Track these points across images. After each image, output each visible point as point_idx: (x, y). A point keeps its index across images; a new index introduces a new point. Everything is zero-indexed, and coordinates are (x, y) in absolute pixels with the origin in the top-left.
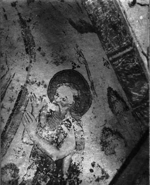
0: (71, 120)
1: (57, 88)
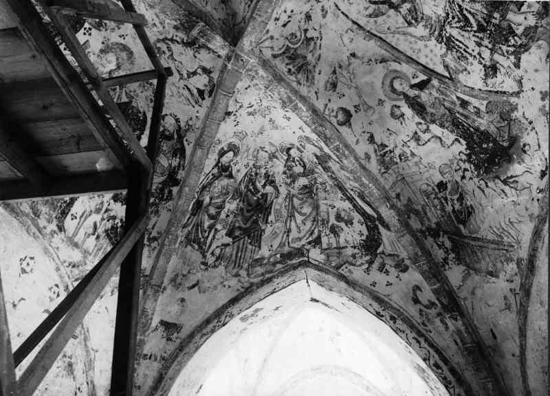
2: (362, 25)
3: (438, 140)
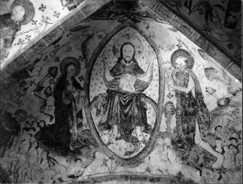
0: (188, 73)
1: (175, 61)
2: (109, 43)
3: (42, 104)
